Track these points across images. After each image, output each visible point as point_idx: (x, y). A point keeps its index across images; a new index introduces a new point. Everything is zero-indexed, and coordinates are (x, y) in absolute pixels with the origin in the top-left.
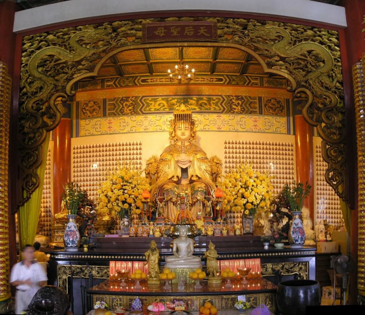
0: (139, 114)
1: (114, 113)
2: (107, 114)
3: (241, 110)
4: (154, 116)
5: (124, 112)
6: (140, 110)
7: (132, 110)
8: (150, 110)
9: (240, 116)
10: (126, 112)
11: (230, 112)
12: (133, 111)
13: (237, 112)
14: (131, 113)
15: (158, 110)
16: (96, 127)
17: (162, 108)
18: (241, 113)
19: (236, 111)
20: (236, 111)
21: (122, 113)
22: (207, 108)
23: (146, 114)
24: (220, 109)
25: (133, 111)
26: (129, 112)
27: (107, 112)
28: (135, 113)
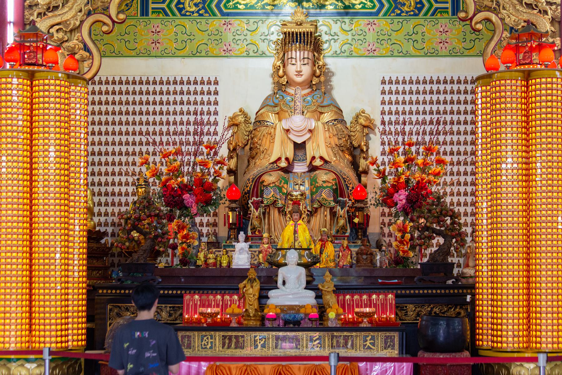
0: (215, 15)
1: (163, 9)
2: (150, 11)
3: (416, 8)
4: (244, 19)
5: (184, 8)
6: (218, 6)
7: (201, 6)
8: (236, 8)
9: (414, 21)
10: (188, 9)
11: (393, 12)
12: (204, 8)
13: (407, 12)
14: (198, 12)
15: (252, 7)
16: (127, 37)
17: (259, 4)
18: (415, 15)
19: (406, 9)
20: (406, 9)
21: (180, 10)
22: (347, 4)
23: (228, 14)
24: (374, 7)
25: (204, 8)
26: (194, 9)
27: (151, 6)
28: (206, 12)
